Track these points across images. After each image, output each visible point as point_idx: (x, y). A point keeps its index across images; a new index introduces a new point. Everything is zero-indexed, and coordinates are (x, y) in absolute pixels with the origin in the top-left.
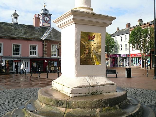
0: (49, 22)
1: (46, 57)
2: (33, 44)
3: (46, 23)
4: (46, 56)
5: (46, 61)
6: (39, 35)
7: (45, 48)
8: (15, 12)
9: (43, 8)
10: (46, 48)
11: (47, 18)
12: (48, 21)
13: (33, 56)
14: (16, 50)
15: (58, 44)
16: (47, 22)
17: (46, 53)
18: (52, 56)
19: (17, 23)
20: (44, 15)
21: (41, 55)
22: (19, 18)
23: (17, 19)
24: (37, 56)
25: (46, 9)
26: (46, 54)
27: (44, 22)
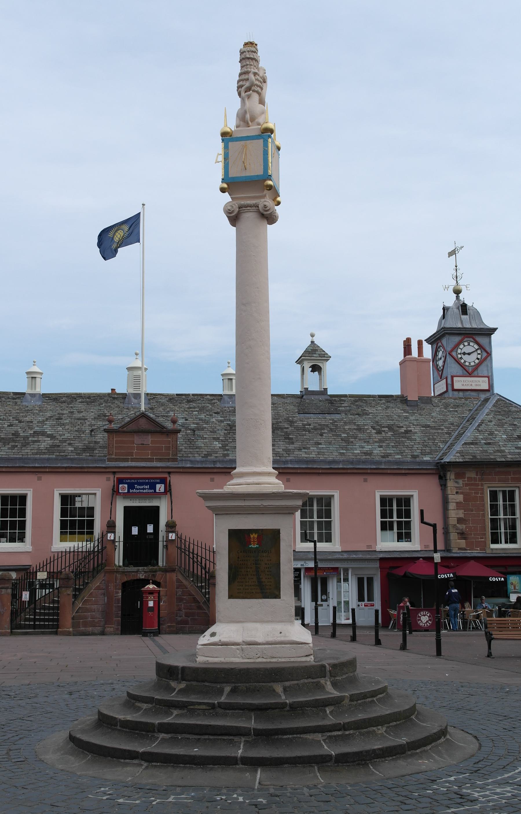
0: (482, 370)
1: (460, 549)
2: (404, 488)
3: (470, 374)
7: (452, 506)
8: (312, 342)
9: (450, 301)
10: (459, 505)
12: (477, 366)
22: (328, 367)
23: (320, 373)
26: (462, 535)
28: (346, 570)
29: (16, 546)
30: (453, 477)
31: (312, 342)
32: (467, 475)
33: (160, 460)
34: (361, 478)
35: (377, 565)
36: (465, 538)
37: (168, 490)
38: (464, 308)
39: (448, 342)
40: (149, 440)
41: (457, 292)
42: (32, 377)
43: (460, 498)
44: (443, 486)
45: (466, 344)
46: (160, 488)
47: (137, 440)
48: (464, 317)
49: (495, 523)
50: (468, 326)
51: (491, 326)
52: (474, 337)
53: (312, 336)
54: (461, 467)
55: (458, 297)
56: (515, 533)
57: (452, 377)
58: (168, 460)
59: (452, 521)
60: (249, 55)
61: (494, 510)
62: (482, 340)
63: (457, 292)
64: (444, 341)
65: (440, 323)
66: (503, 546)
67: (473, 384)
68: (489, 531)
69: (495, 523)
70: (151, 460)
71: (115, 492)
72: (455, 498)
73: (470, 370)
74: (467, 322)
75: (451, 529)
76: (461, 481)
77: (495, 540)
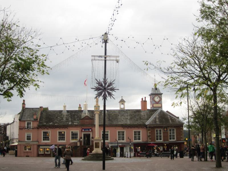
4: (150, 140)
6: (145, 119)
7: (148, 133)
8: (122, 98)
10: (150, 133)
11: (157, 99)
13: (137, 141)
14: (121, 135)
16: (157, 103)
17: (150, 137)
19: (124, 109)
20: (154, 96)
21: (145, 140)
22: (126, 104)
24: (141, 141)
26: (150, 139)
27: (154, 102)
28: (127, 146)
29: (64, 141)
35: (133, 145)
37: (92, 131)
38: (156, 89)
40: (88, 121)
42: (65, 107)
46: (90, 130)
48: (156, 91)
49: (157, 136)
50: (157, 93)
51: (162, 93)
53: (122, 97)
61: (157, 134)
62: (159, 96)
66: (159, 141)
69: (157, 136)
71: (82, 131)
74: (156, 92)
77: (157, 139)
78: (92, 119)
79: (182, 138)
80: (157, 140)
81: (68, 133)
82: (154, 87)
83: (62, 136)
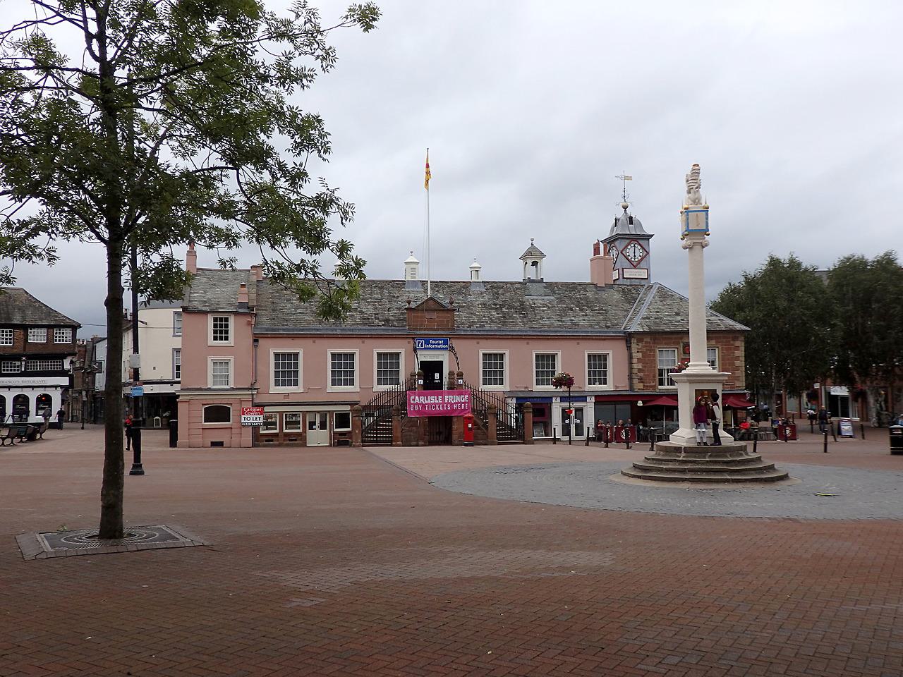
0: (643, 264)
1: (639, 389)
3: (635, 267)
5: (640, 403)
7: (635, 361)
8: (532, 244)
9: (620, 213)
11: (634, 251)
15: (678, 343)
18: (660, 387)
21: (624, 386)
22: (544, 263)
23: (536, 267)
24: (609, 387)
25: (631, 218)
26: (641, 380)
27: (627, 264)
30: (635, 341)
31: (532, 244)
32: (645, 340)
33: (443, 330)
34: (575, 342)
36: (642, 382)
39: (620, 245)
40: (435, 315)
41: (625, 208)
43: (640, 355)
44: (629, 348)
45: (632, 245)
47: (428, 315)
52: (640, 242)
54: (640, 335)
55: (625, 211)
56: (659, 376)
57: (623, 269)
58: (449, 329)
59: (635, 371)
60: (696, 171)
63: (625, 208)
64: (617, 243)
65: (612, 230)
66: (666, 387)
67: (637, 274)
68: (657, 378)
70: (437, 330)
72: (637, 356)
73: (635, 264)
74: (632, 230)
75: (634, 376)
76: (640, 344)
77: (661, 383)
78: (448, 310)
79: (738, 380)
80: (660, 385)
81: (366, 356)
82: (620, 213)
83: (343, 368)
